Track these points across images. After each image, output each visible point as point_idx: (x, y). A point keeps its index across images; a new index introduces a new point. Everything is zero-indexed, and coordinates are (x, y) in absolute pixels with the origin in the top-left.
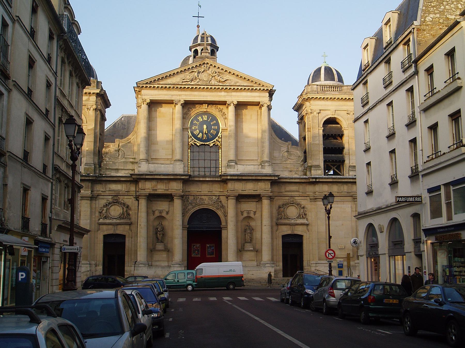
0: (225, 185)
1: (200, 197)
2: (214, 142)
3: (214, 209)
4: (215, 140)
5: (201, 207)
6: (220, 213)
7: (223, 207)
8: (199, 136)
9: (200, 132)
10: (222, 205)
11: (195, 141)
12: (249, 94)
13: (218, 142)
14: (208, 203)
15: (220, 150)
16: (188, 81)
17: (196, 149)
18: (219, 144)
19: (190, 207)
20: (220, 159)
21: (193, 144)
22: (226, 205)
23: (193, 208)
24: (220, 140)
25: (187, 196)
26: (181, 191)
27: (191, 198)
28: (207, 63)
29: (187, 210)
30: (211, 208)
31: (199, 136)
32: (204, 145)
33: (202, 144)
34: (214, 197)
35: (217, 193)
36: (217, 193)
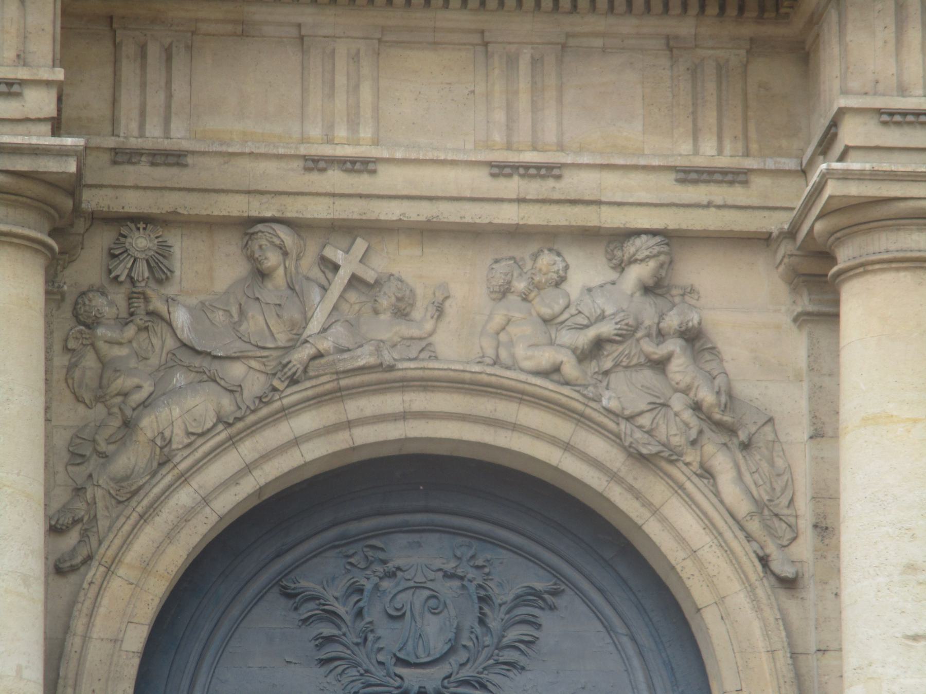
0: (772, 73)
1: (350, 263)
3: (582, 459)
5: (380, 423)
6: (682, 530)
7: (727, 422)
10: (730, 399)
14: (475, 353)
19: (188, 408)
22: (789, 403)
23: (234, 427)
25: (141, 242)
26: (40, 102)
27: (203, 273)
29: (132, 458)
30: (534, 439)
34: (585, 272)
35: (639, 187)
36: (641, 200)
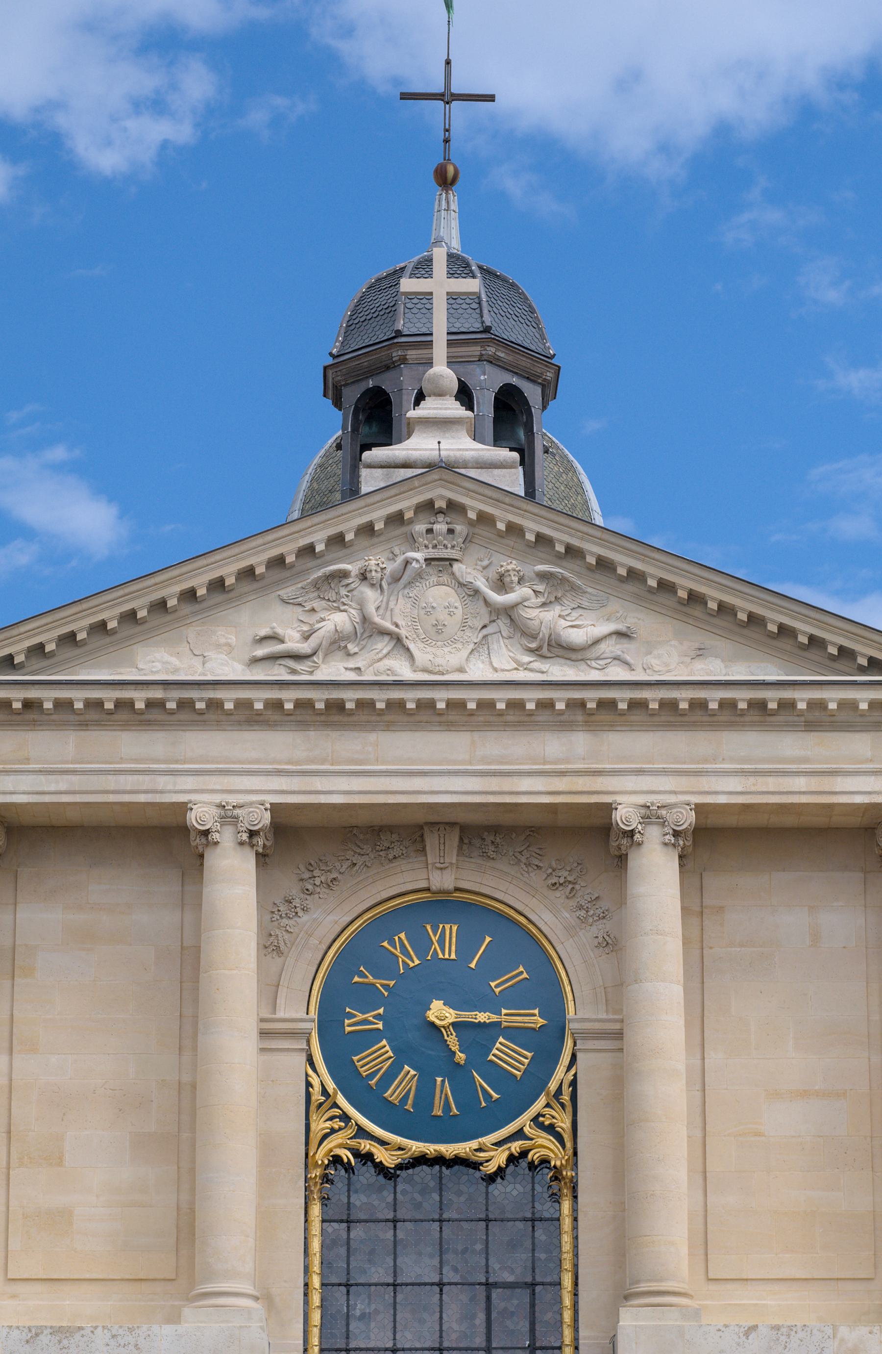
2: (519, 1134)
4: (524, 1120)
8: (393, 1094)
9: (403, 1055)
11: (361, 1132)
12: (789, 745)
13: (545, 1140)
15: (566, 1206)
16: (305, 648)
17: (371, 1199)
18: (558, 1157)
20: (567, 1280)
21: (346, 1155)
24: (563, 1123)
28: (453, 507)
31: (393, 1094)
32: (439, 1160)
33: (421, 1160)
